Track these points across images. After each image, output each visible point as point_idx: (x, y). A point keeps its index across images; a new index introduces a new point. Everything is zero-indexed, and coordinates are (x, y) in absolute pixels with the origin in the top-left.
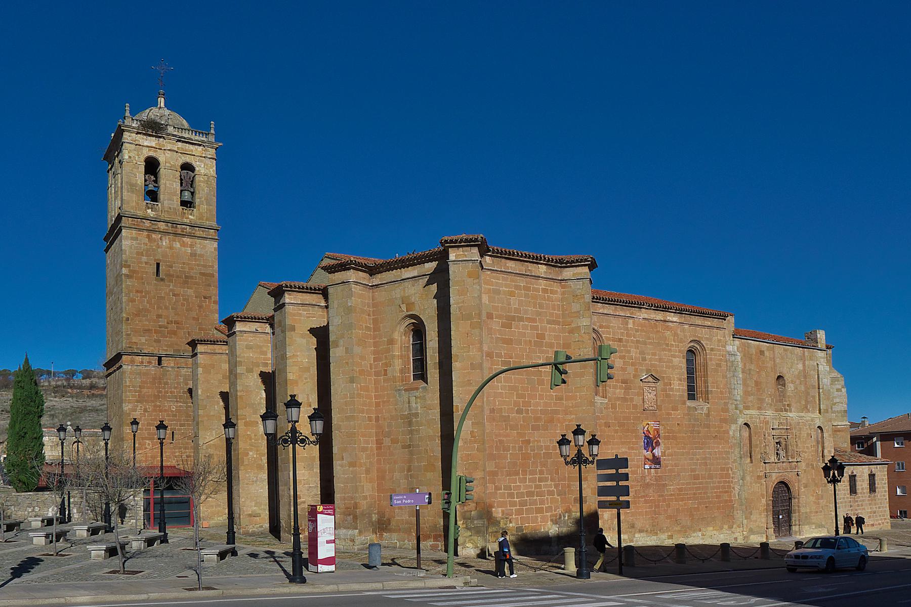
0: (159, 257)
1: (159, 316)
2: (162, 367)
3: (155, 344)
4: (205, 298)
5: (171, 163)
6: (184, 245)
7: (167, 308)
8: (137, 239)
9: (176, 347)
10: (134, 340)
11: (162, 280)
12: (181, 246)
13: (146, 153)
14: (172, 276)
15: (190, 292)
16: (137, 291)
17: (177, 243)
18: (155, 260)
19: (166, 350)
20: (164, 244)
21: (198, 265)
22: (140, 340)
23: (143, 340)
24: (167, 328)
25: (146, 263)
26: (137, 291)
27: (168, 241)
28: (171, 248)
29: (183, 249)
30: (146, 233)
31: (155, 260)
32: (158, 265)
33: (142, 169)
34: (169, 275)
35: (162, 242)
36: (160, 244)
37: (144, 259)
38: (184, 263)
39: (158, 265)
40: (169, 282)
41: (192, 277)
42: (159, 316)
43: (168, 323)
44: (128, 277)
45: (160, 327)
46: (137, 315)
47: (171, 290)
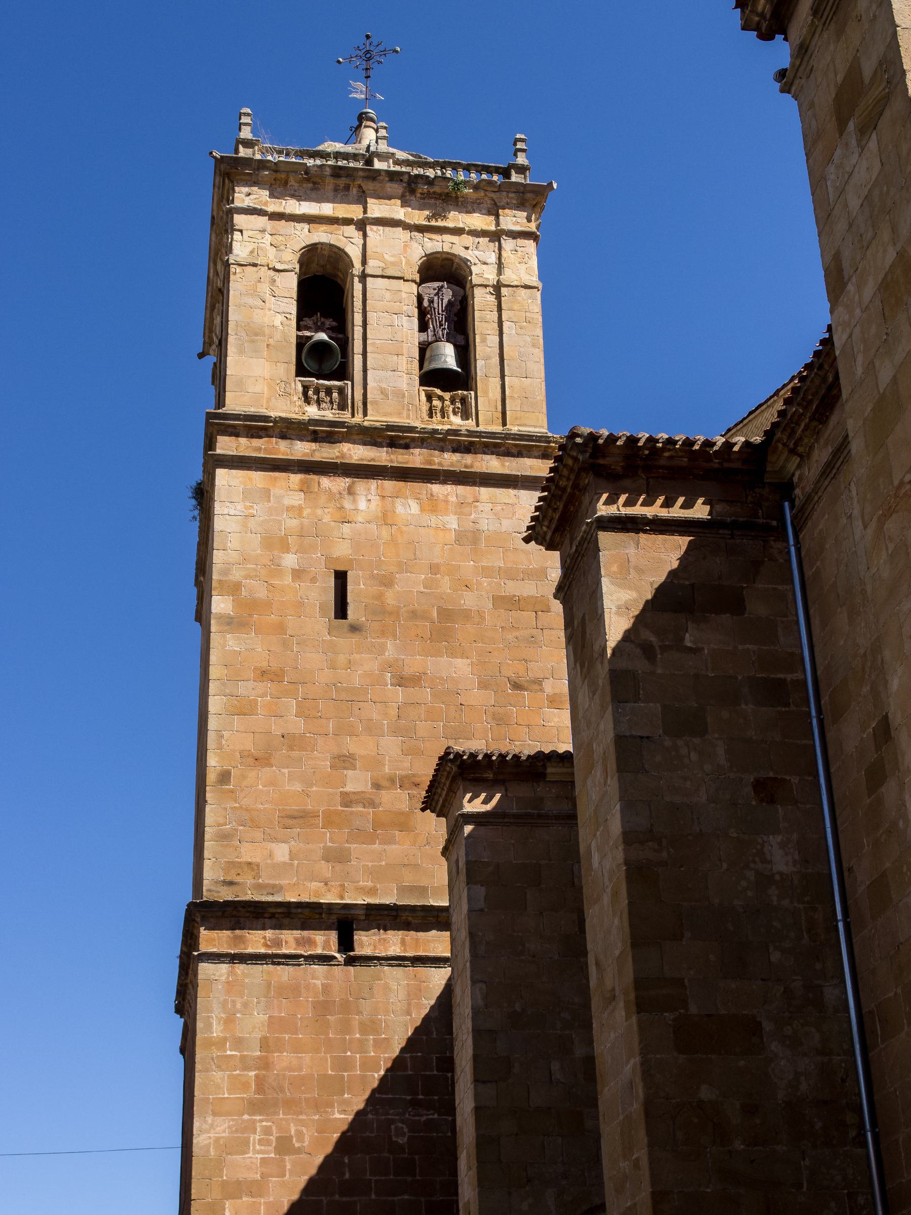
0: (342, 551)
1: (344, 761)
2: (351, 961)
3: (325, 869)
4: (517, 686)
5: (386, 256)
6: (432, 506)
7: (372, 729)
8: (266, 494)
9: (409, 879)
10: (248, 853)
11: (355, 629)
12: (422, 510)
13: (304, 236)
14: (395, 613)
15: (461, 667)
16: (263, 674)
17: (411, 502)
18: (329, 559)
19: (373, 891)
20: (362, 505)
21: (487, 572)
22: (271, 855)
23: (281, 852)
24: (372, 804)
25: (297, 574)
26: (263, 673)
27: (376, 500)
28: (386, 518)
29: (434, 520)
30: (296, 479)
31: (329, 559)
32: (341, 578)
33: (290, 283)
34: (380, 611)
35: (354, 501)
36: (347, 504)
37: (290, 560)
38: (434, 569)
39: (341, 578)
40: (383, 633)
41: (466, 615)
42: (344, 761)
43: (377, 786)
44: (229, 624)
45: (348, 800)
46: (261, 760)
47: (390, 665)
